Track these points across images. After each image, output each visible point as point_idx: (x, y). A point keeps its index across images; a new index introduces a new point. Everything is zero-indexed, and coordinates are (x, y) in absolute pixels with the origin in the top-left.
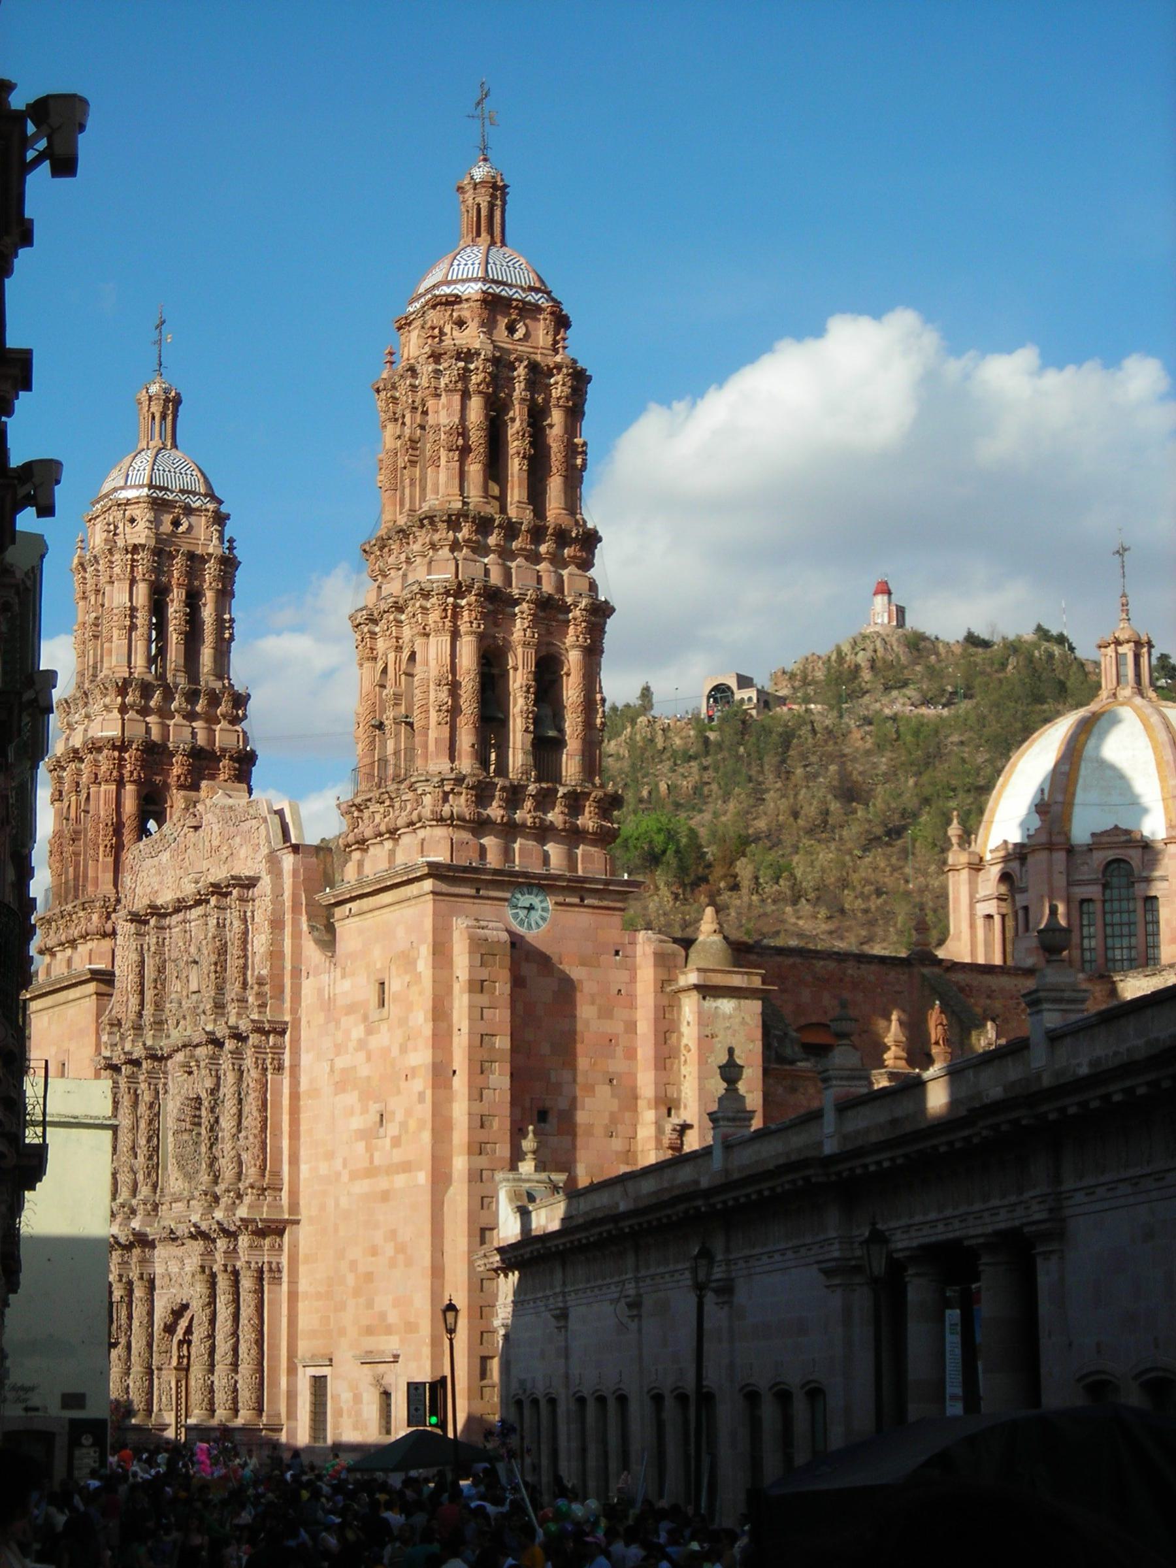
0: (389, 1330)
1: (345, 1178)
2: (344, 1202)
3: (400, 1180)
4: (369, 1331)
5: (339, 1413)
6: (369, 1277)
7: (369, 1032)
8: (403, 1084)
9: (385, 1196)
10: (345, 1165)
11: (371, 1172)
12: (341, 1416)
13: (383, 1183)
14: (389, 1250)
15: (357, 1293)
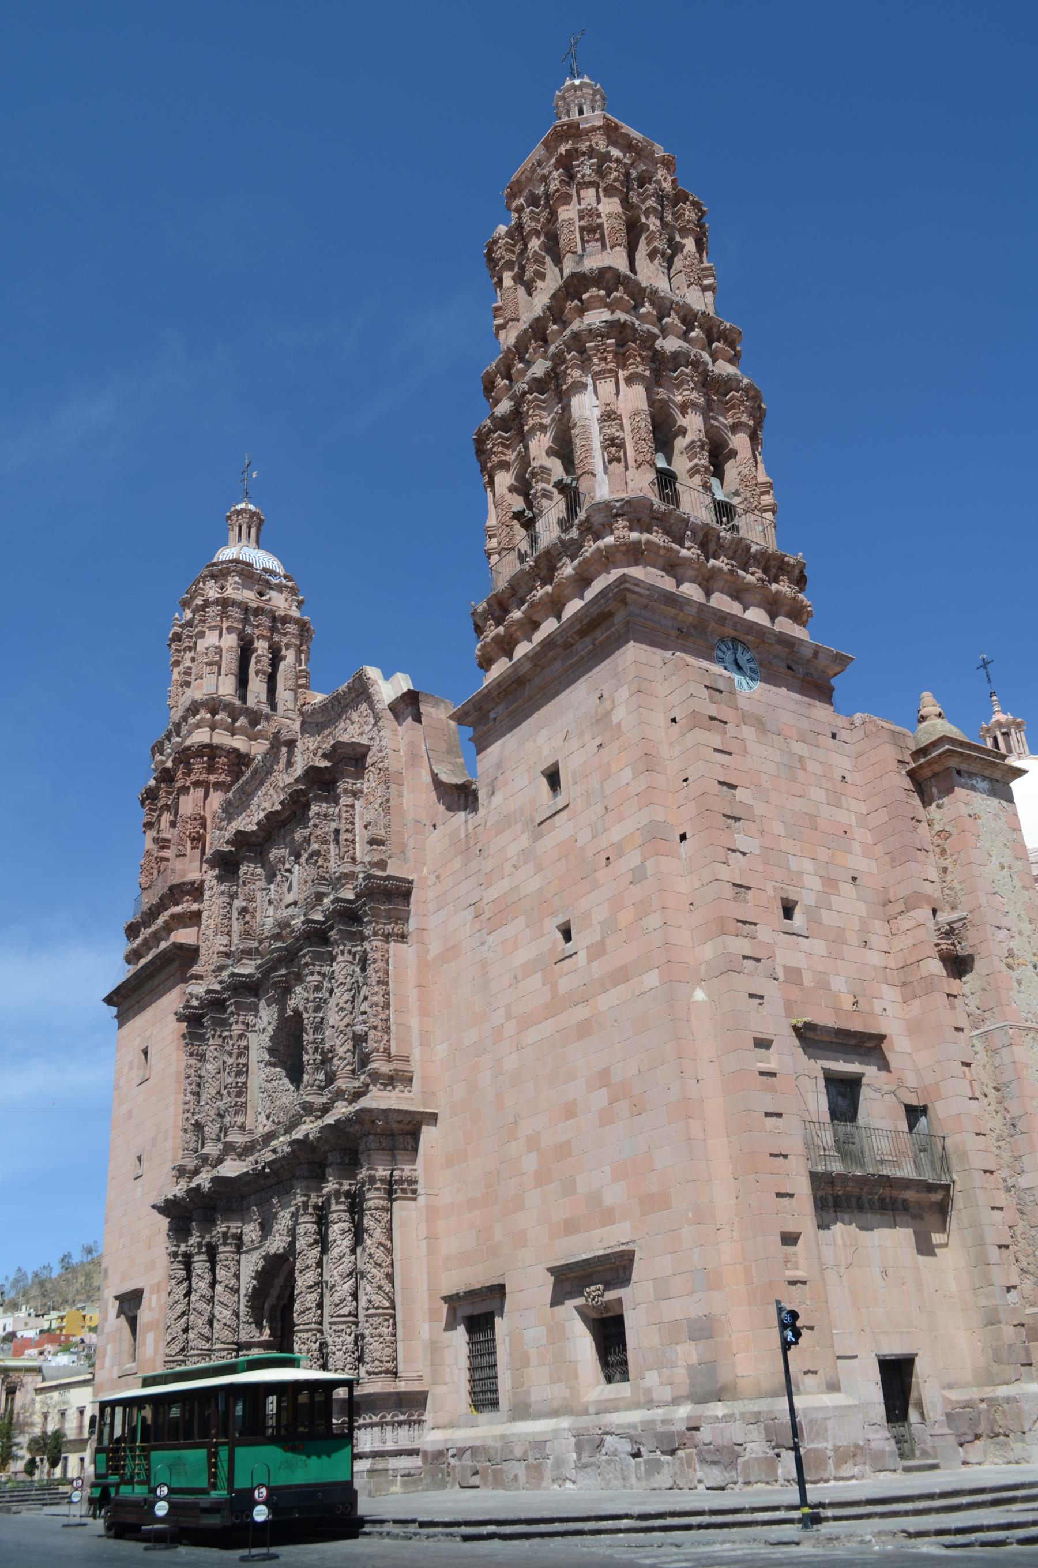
0: (608, 1217)
1: (511, 1028)
2: (511, 1062)
3: (606, 1001)
4: (570, 1227)
5: (521, 1362)
6: (563, 1150)
7: (536, 838)
8: (602, 874)
9: (584, 1029)
10: (509, 1017)
11: (555, 1006)
12: (526, 1363)
13: (580, 1013)
14: (600, 1098)
15: (541, 1178)
